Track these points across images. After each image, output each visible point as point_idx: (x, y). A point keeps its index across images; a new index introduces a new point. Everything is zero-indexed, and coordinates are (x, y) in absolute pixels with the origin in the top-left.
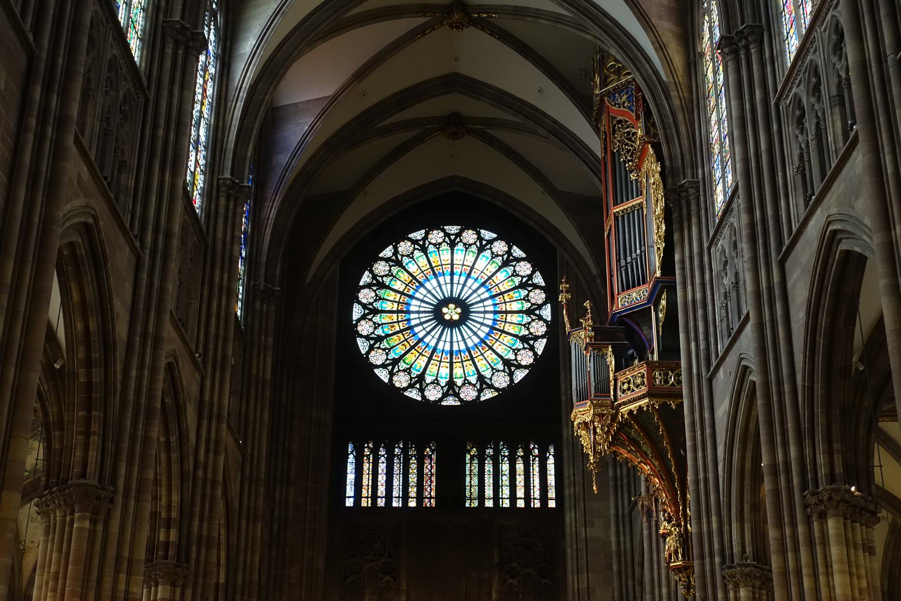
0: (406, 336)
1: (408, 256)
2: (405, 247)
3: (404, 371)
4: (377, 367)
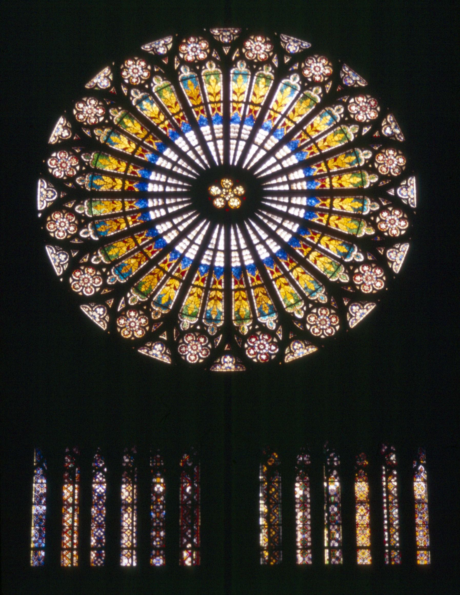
0: (139, 241)
1: (141, 87)
3: (138, 308)
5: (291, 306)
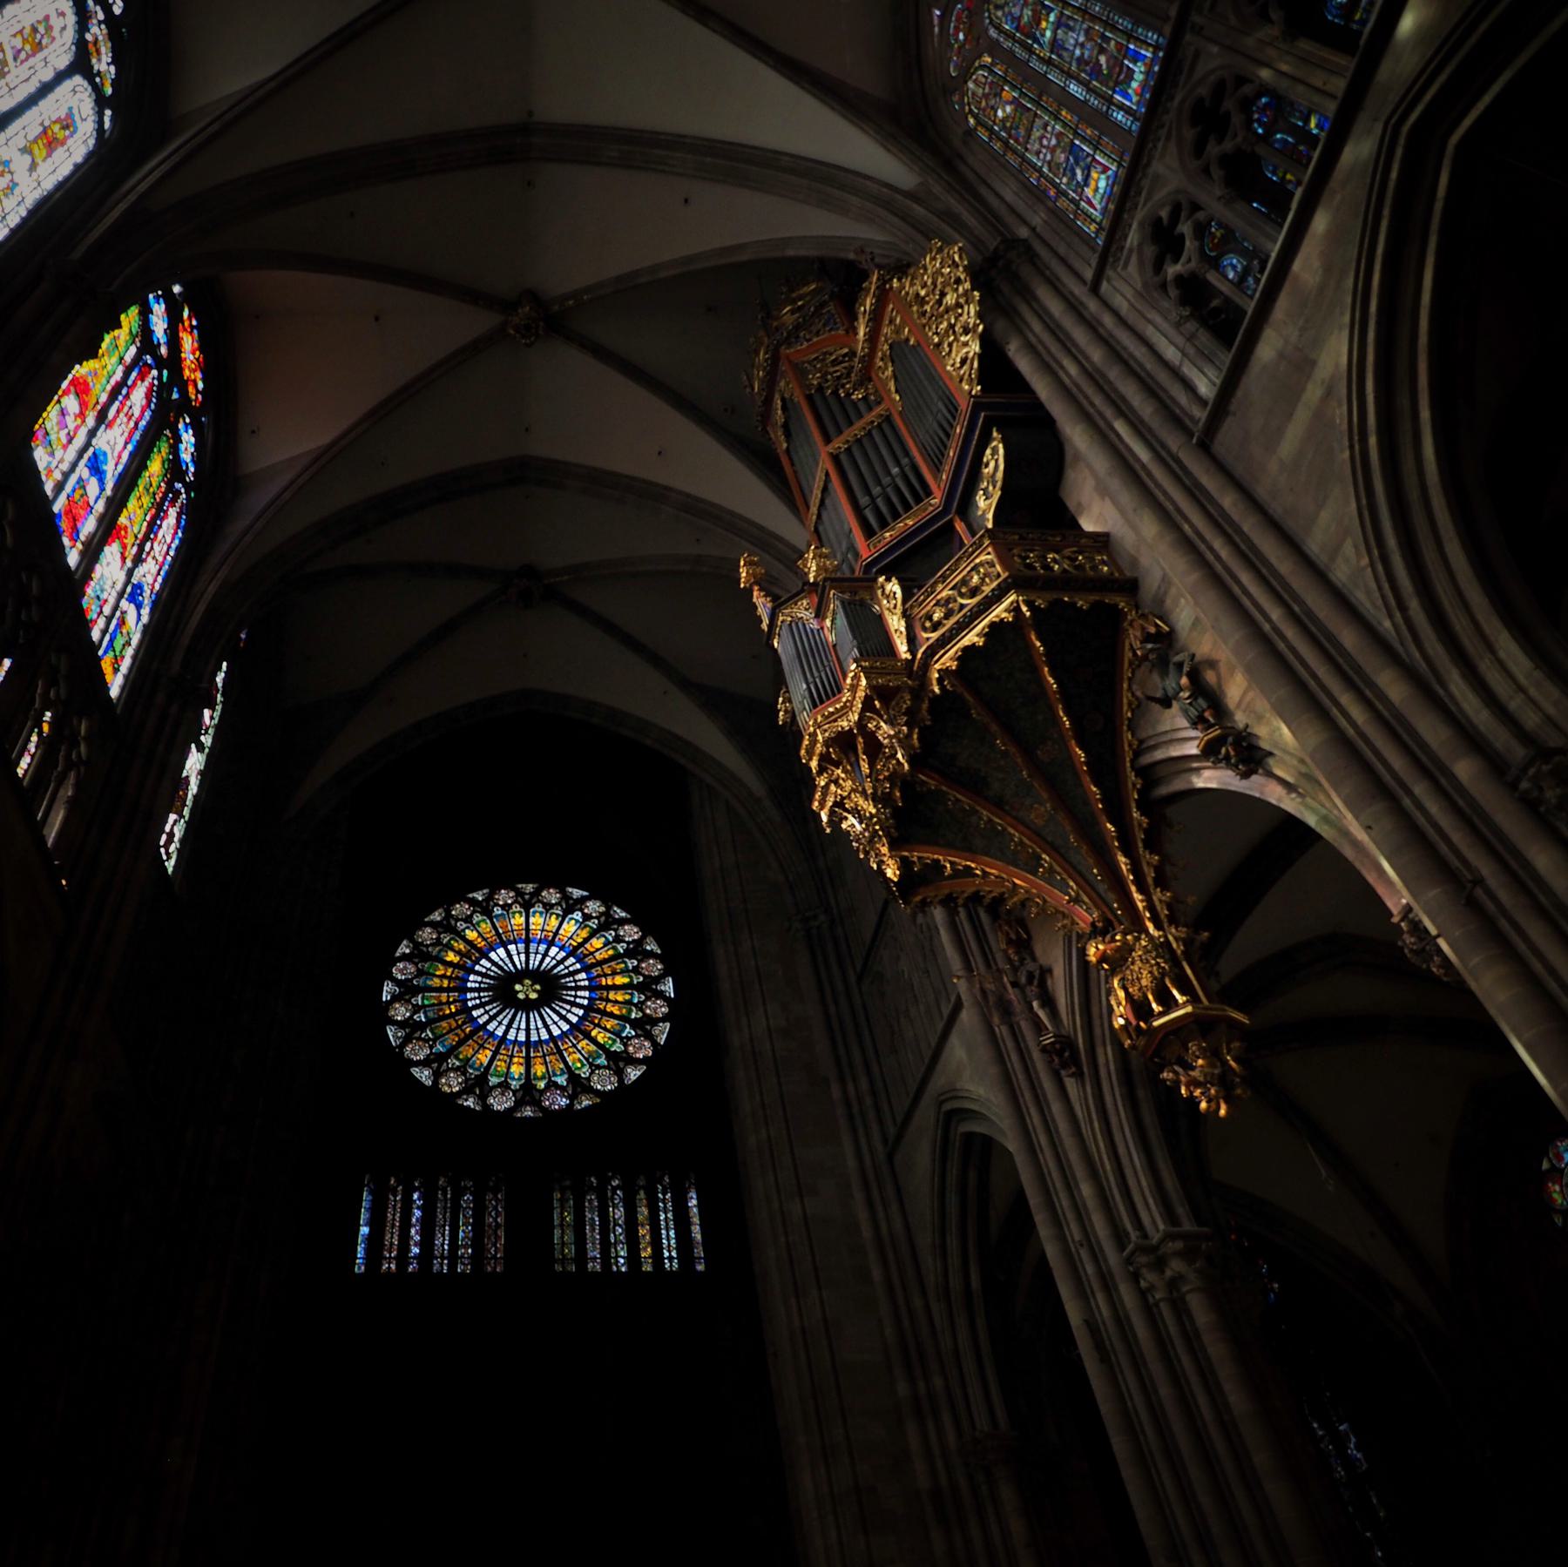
2: (460, 909)
5: (579, 1068)
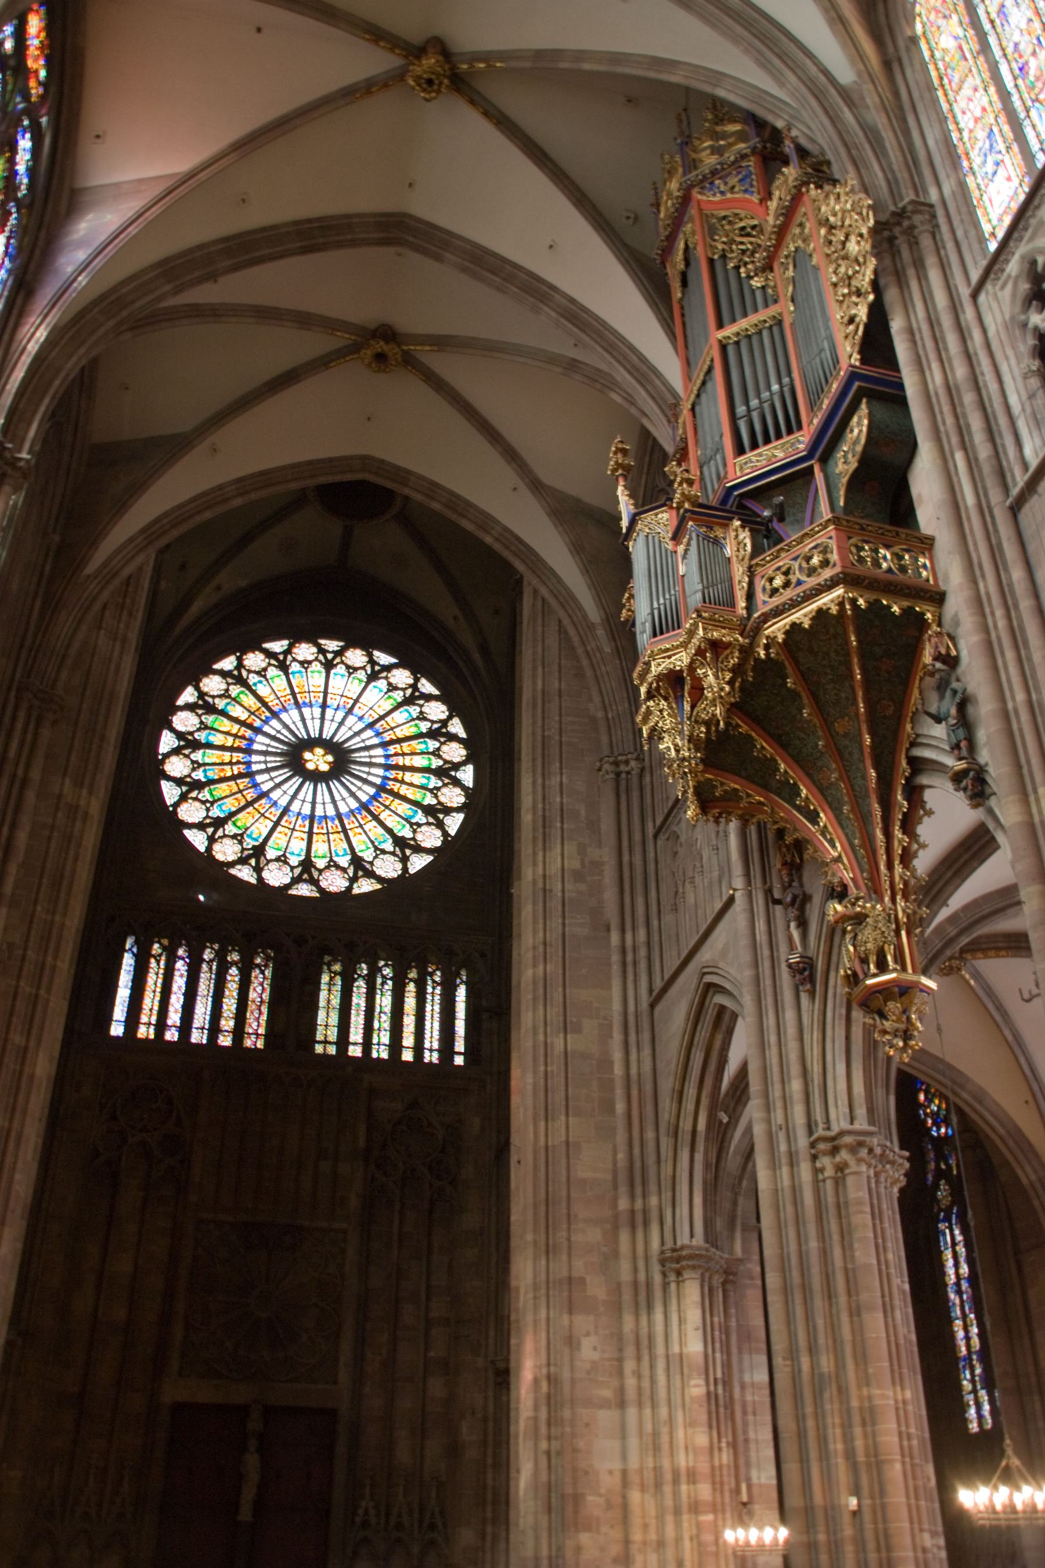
1: (258, 673)
2: (254, 660)
3: (234, 837)
4: (191, 826)
